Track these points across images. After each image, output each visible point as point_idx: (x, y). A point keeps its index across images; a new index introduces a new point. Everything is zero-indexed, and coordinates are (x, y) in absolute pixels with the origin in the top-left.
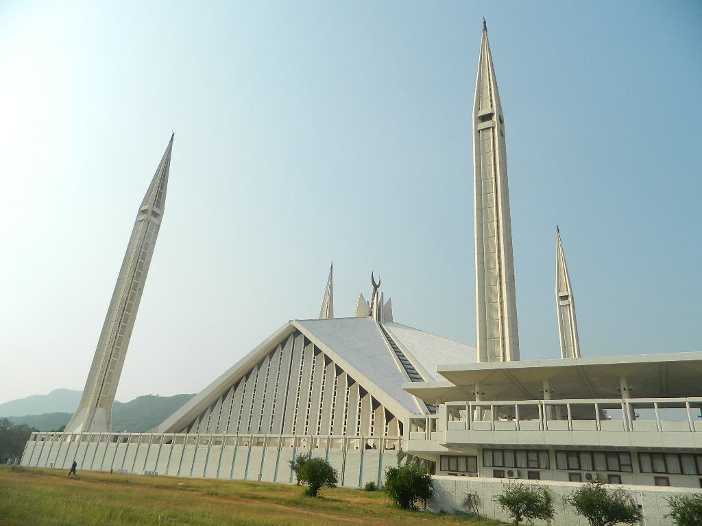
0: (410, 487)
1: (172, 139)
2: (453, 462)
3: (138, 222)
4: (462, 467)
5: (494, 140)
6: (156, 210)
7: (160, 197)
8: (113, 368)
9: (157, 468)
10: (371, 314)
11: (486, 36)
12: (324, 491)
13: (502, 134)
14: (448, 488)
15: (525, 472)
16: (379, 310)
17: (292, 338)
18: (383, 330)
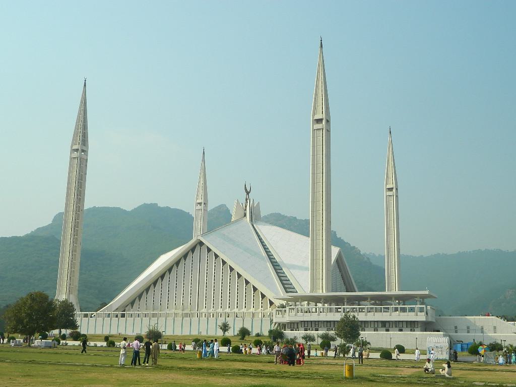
0: (276, 335)
1: (85, 85)
2: (292, 324)
3: (72, 159)
4: (296, 327)
5: (323, 137)
6: (84, 148)
7: (85, 138)
8: (74, 269)
9: (127, 331)
10: (245, 215)
11: (322, 52)
12: (247, 338)
13: (328, 131)
14: (287, 335)
15: (314, 329)
16: (251, 212)
17: (198, 247)
18: (255, 230)
